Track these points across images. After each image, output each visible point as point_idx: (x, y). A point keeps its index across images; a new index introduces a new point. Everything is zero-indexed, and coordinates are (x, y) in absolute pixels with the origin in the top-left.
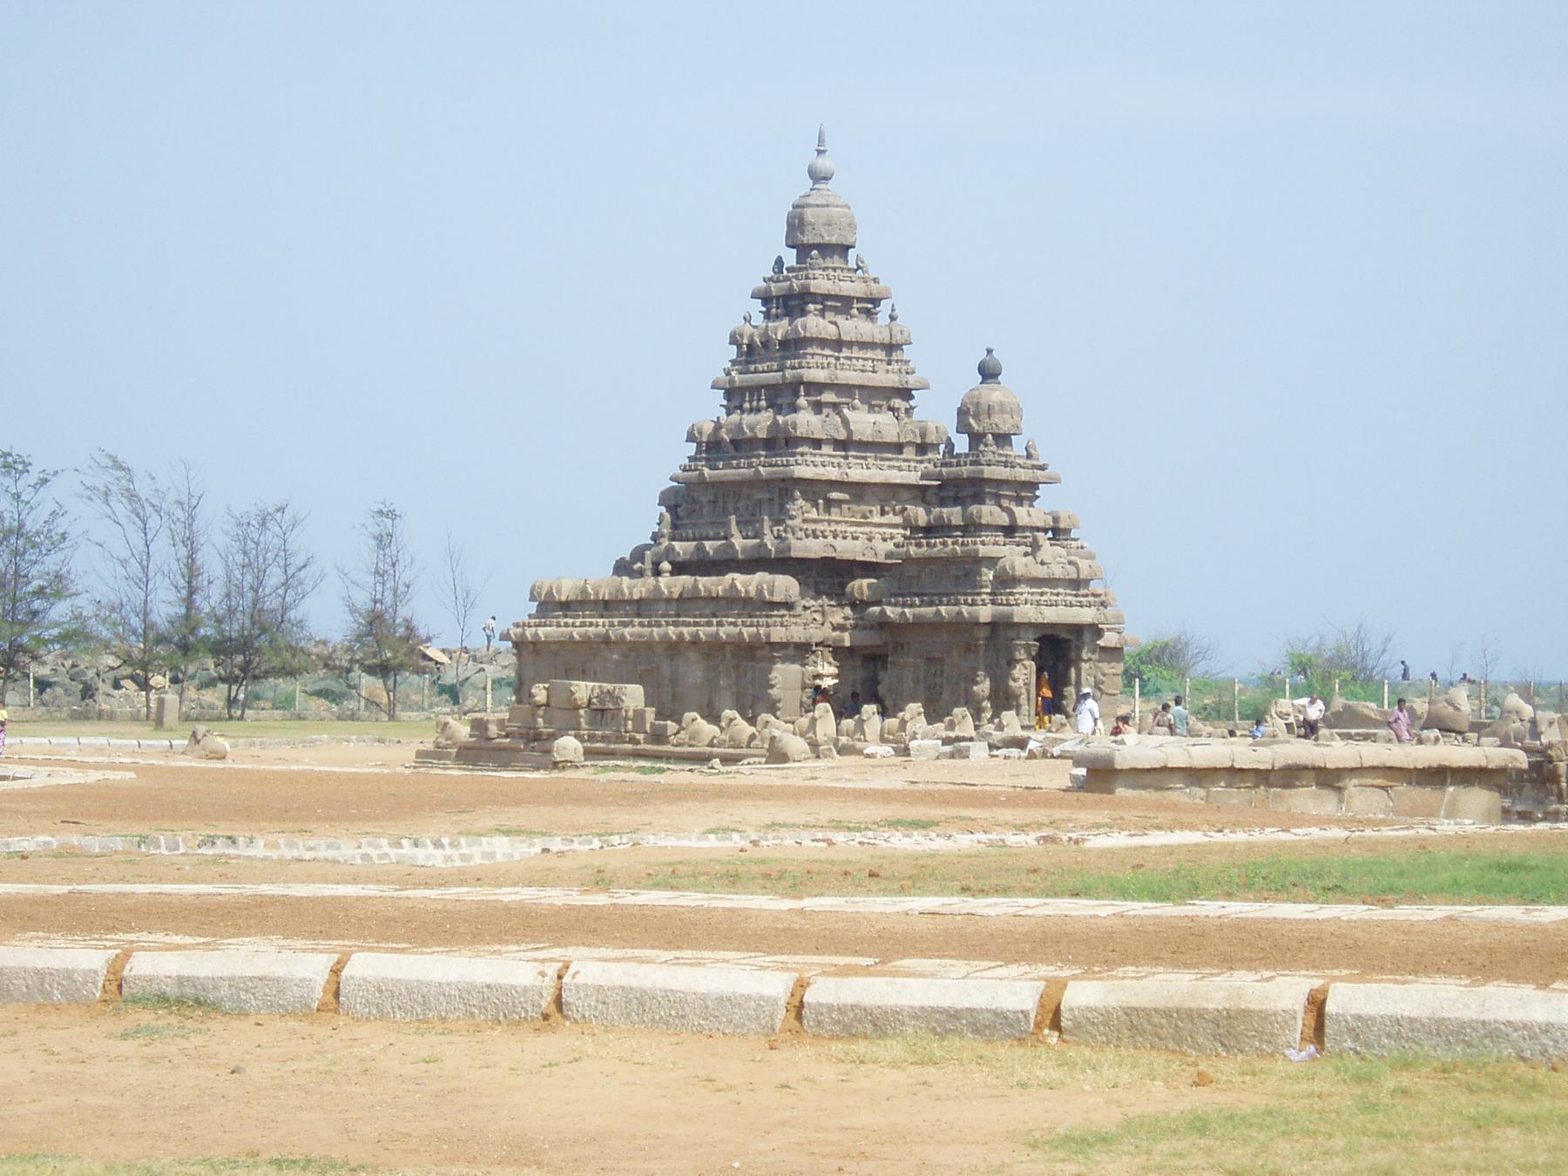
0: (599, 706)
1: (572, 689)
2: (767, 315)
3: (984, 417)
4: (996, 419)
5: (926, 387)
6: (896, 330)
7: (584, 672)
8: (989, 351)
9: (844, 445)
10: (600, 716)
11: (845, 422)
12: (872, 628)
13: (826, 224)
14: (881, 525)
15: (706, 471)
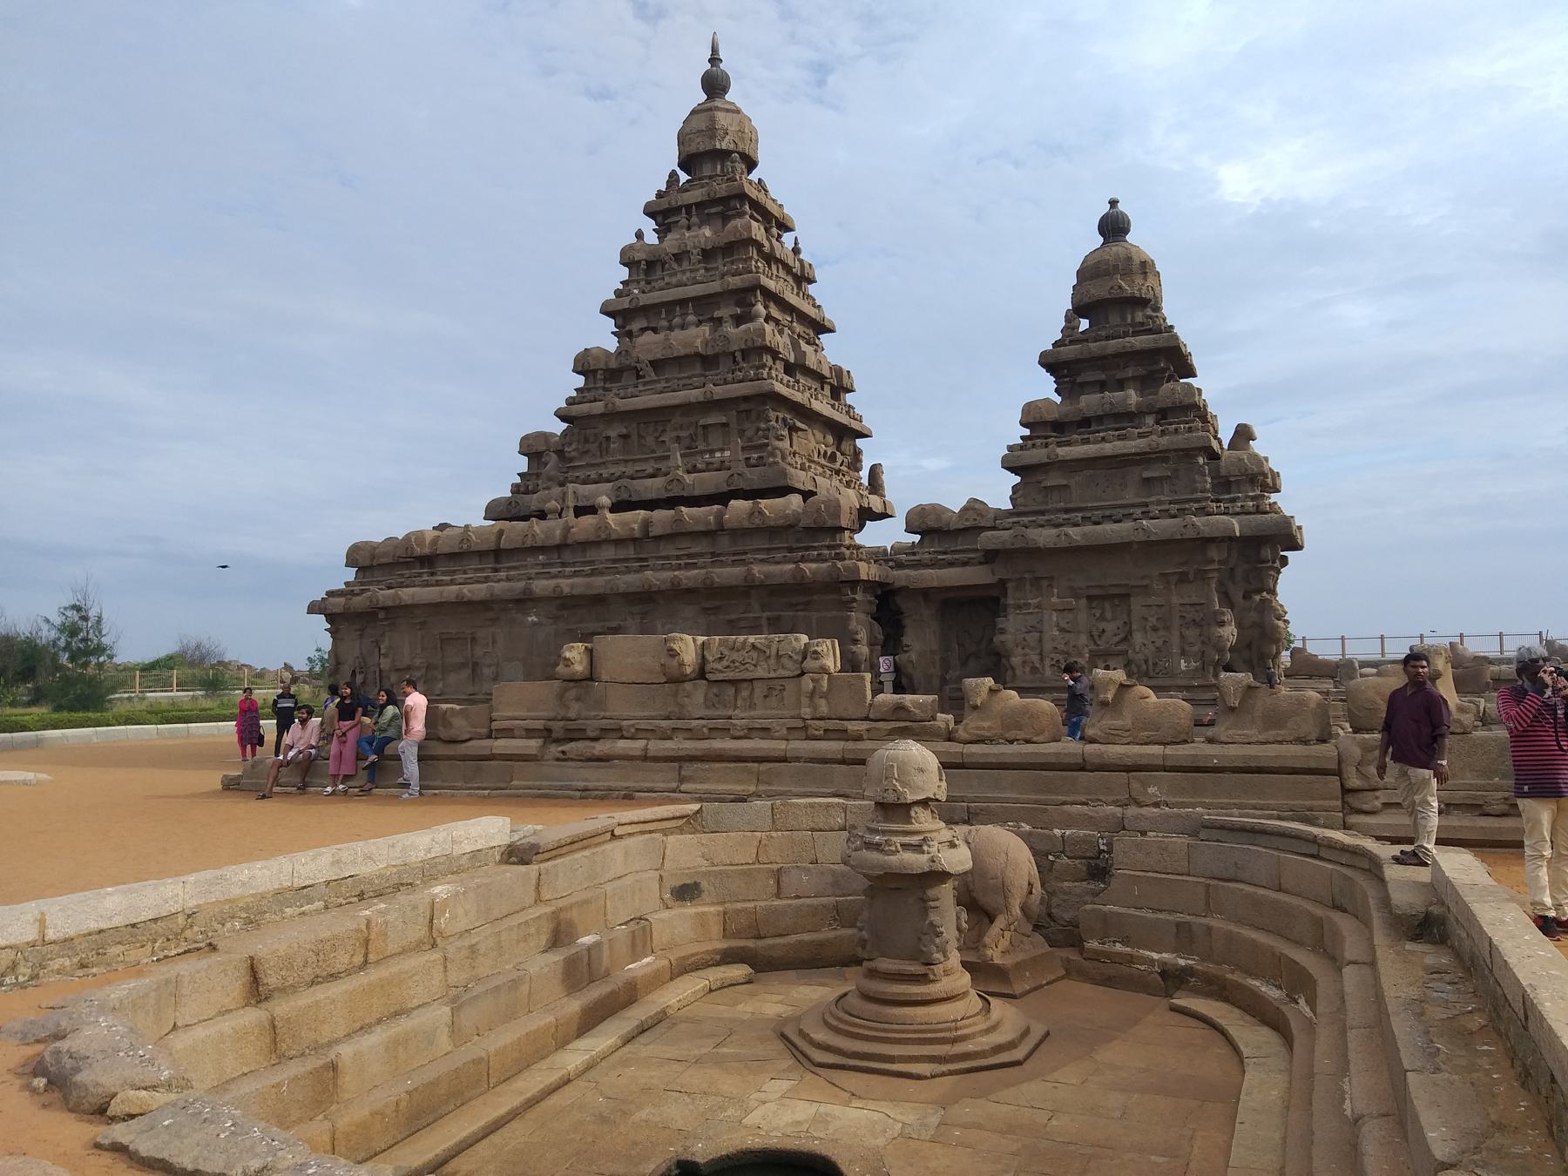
0: (730, 675)
1: (675, 647)
2: (662, 231)
3: (1139, 280)
4: (1150, 281)
5: (831, 331)
6: (807, 266)
7: (473, 640)
8: (1113, 203)
9: (789, 369)
10: (731, 691)
11: (795, 346)
12: (965, 564)
13: (740, 131)
14: (823, 466)
15: (617, 401)
